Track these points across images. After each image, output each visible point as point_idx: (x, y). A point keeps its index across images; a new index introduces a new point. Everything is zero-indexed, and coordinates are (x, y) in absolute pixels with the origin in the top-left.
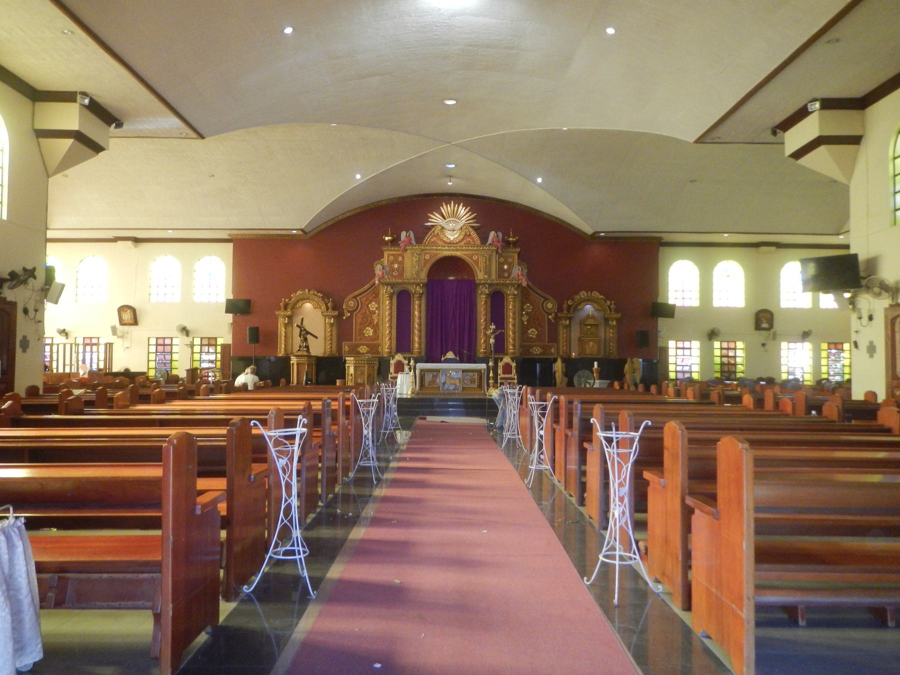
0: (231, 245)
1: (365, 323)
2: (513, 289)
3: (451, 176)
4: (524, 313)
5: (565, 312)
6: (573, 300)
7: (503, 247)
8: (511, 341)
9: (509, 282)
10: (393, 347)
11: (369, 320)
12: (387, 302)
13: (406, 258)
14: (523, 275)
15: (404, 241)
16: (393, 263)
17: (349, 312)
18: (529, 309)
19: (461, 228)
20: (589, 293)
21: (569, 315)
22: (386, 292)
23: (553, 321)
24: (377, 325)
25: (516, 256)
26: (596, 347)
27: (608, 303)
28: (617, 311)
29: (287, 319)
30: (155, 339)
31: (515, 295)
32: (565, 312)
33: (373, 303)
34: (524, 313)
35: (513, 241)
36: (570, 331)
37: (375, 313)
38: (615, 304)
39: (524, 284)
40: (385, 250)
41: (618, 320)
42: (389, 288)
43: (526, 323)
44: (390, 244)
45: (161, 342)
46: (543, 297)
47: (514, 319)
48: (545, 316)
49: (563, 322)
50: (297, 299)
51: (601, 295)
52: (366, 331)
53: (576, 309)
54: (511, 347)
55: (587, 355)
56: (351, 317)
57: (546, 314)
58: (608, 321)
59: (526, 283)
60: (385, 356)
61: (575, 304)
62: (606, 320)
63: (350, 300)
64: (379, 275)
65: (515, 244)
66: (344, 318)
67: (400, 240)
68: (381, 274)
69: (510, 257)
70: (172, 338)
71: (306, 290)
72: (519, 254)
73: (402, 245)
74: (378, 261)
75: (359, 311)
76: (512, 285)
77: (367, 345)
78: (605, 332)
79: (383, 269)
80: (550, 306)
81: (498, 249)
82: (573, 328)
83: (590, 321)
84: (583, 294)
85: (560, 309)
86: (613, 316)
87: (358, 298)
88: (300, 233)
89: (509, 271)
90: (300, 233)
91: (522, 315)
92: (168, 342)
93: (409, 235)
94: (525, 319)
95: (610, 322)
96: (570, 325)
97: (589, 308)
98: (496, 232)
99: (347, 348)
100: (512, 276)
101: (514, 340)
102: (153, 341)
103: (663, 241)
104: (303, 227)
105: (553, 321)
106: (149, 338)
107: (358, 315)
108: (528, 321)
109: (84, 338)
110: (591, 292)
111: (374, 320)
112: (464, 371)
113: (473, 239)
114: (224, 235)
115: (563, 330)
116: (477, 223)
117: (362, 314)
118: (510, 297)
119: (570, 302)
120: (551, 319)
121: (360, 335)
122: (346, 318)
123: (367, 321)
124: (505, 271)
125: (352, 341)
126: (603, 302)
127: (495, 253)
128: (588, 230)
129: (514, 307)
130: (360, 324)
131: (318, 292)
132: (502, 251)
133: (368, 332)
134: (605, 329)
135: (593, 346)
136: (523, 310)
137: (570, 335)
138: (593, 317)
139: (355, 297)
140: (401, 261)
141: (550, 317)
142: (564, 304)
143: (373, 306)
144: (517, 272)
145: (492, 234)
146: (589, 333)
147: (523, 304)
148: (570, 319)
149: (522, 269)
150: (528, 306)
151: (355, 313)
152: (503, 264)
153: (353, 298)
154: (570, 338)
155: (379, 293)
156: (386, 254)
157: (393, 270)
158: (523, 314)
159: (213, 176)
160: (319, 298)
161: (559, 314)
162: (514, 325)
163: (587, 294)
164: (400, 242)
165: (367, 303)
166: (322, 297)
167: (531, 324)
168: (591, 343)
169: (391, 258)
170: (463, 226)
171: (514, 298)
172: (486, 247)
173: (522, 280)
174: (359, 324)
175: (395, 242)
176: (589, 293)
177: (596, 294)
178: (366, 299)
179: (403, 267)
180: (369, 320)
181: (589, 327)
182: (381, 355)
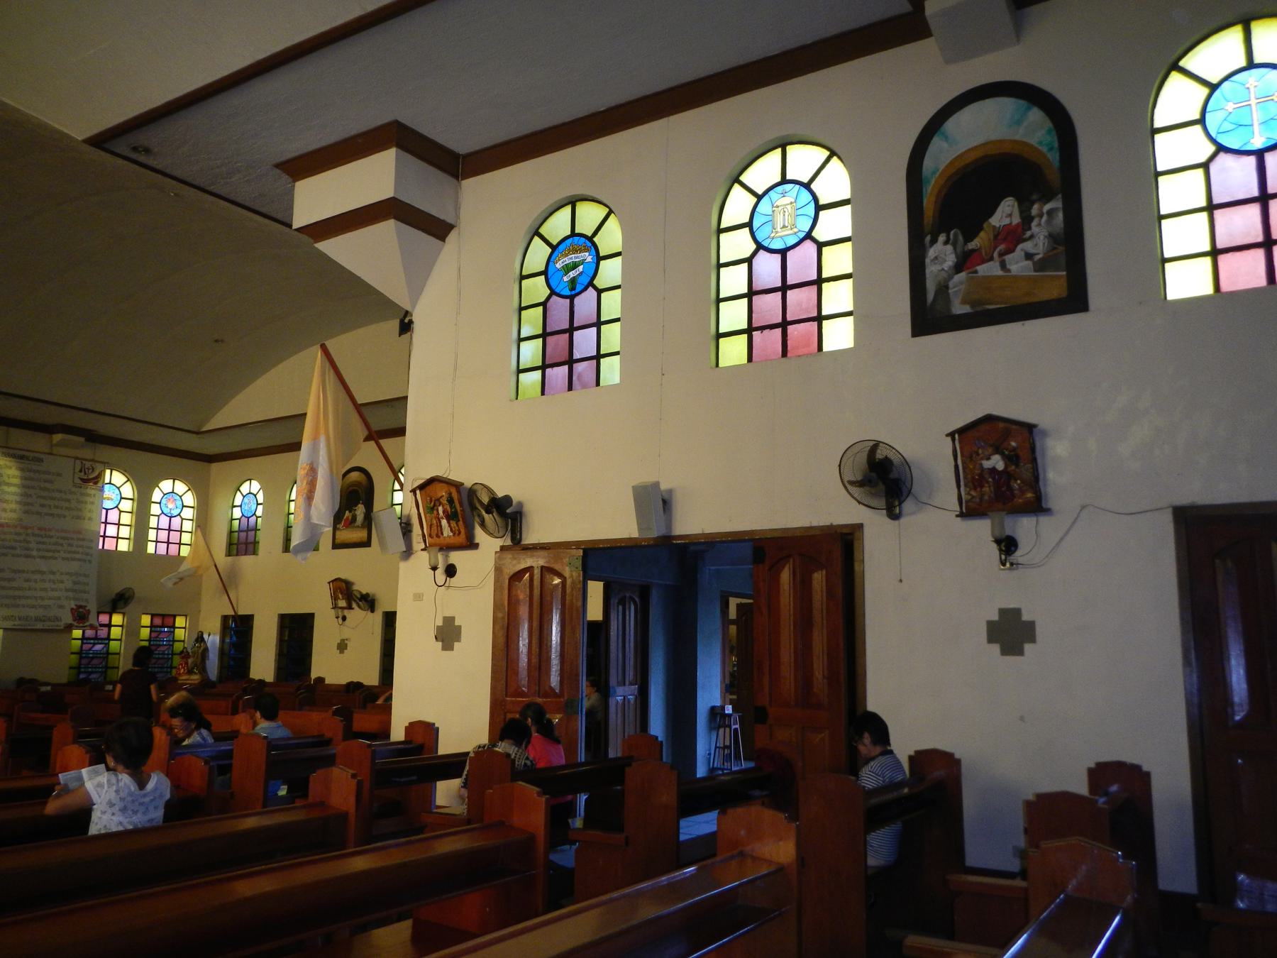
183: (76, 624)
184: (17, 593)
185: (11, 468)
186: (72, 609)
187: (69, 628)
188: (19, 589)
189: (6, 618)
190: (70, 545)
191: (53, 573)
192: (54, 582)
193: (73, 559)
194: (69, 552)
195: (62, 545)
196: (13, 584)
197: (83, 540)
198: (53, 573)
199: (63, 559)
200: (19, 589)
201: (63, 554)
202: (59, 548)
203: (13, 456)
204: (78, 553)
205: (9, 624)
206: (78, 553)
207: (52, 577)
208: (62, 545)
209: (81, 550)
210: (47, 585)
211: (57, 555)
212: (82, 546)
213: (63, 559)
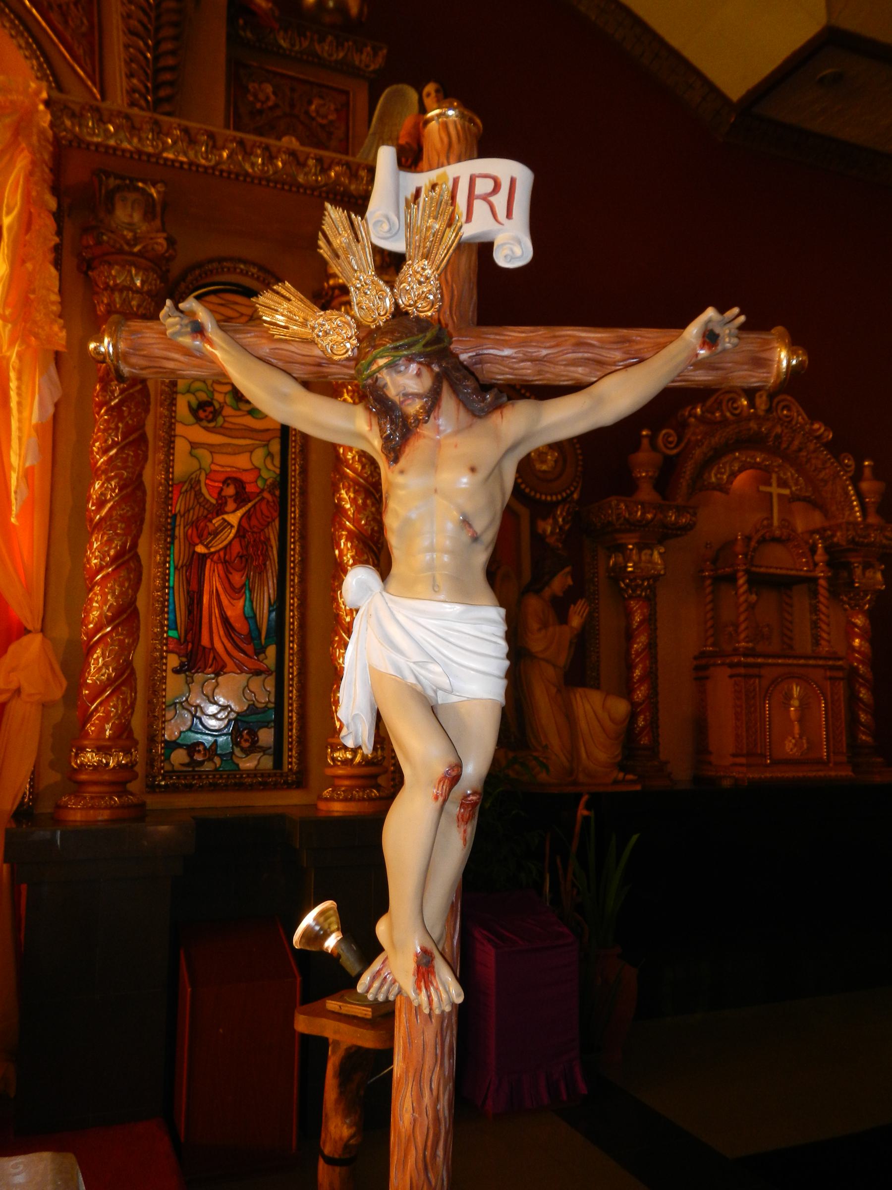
6: (681, 427)
21: (672, 517)
32: (646, 493)
38: (877, 474)
51: (813, 418)
55: (776, 762)
115: (629, 615)
120: (551, 541)
141: (546, 527)
142: (637, 447)
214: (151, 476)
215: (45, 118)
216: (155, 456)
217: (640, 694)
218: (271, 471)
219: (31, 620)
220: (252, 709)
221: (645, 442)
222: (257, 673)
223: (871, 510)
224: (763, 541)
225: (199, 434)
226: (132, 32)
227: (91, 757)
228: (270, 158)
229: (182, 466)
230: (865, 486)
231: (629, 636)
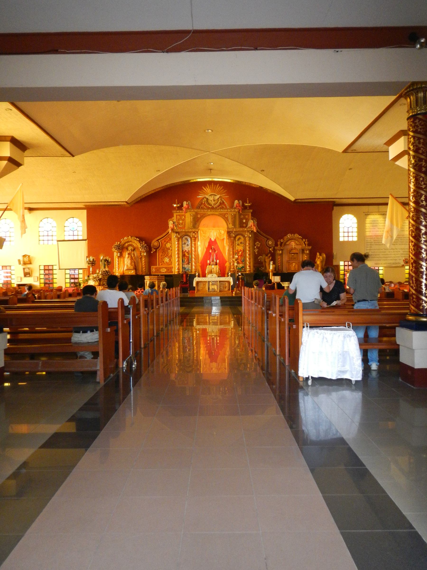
0: (85, 212)
1: (164, 255)
2: (248, 234)
3: (211, 169)
4: (255, 247)
5: (279, 246)
7: (243, 209)
8: (248, 263)
9: (247, 230)
10: (180, 269)
11: (166, 253)
12: (176, 243)
13: (187, 216)
14: (254, 226)
15: (185, 207)
16: (179, 220)
17: (154, 249)
18: (258, 245)
19: (218, 199)
20: (293, 235)
21: (281, 248)
22: (176, 237)
23: (272, 252)
24: (171, 256)
25: (250, 214)
26: (297, 266)
27: (304, 240)
28: (309, 245)
29: (119, 253)
30: (43, 266)
31: (250, 237)
32: (279, 246)
33: (168, 243)
34: (255, 247)
35: (249, 205)
36: (282, 257)
37: (169, 249)
38: (308, 241)
39: (255, 231)
40: (174, 213)
41: (310, 251)
42: (177, 235)
43: (257, 253)
44: (177, 209)
45: (47, 268)
46: (266, 238)
47: (249, 251)
48: (267, 248)
49: (278, 252)
50: (125, 242)
52: (165, 260)
53: (285, 244)
54: (248, 267)
56: (156, 252)
57: (268, 248)
58: (304, 251)
59: (256, 230)
60: (176, 274)
61: (285, 242)
62: (303, 251)
63: (155, 242)
64: (171, 227)
65: (250, 207)
66: (152, 252)
67: (183, 206)
68: (172, 227)
69: (247, 215)
70: (53, 266)
71: (130, 237)
72: (252, 213)
73: (184, 209)
74: (171, 219)
75: (160, 248)
76: (248, 231)
77: (165, 268)
78: (303, 257)
79: (173, 223)
80: (270, 243)
81: (239, 210)
82: (284, 256)
83: (294, 251)
84: (289, 236)
85: (276, 245)
86: (306, 248)
87: (159, 241)
88: (125, 203)
89: (247, 223)
90: (125, 203)
91: (254, 249)
92: (50, 268)
93: (188, 204)
94: (256, 251)
95: (305, 251)
96: (282, 254)
97: (293, 244)
98: (238, 201)
99: (154, 270)
100: (248, 227)
101: (250, 263)
102: (42, 268)
103: (336, 203)
104: (127, 200)
105: (272, 252)
106: (40, 266)
107: (160, 250)
108: (258, 252)
109: (2, 266)
110: (294, 234)
111: (169, 253)
112: (220, 282)
113: (225, 205)
114: (81, 206)
116: (227, 196)
117: (162, 250)
118: (247, 238)
119: (282, 241)
121: (161, 262)
122: (153, 252)
123: (165, 254)
124: (244, 223)
125: (157, 265)
126: (301, 240)
127: (238, 213)
128: (292, 199)
129: (249, 244)
130: (161, 256)
131: (137, 237)
132: (242, 212)
133: (166, 260)
134: (303, 255)
135: (295, 265)
136: (255, 245)
137: (282, 260)
138: (295, 249)
139: (158, 240)
140: (184, 219)
141: (271, 249)
142: (278, 242)
143: (168, 245)
144: (251, 224)
145: (236, 202)
146: (293, 258)
147: (255, 242)
148: (282, 250)
149: (254, 222)
150: (258, 243)
151: (158, 250)
152: (242, 219)
153: (157, 241)
154: (282, 261)
155: (171, 237)
156: (175, 215)
157: (179, 224)
158: (255, 248)
159: (75, 172)
160: (137, 241)
161: (276, 248)
162: (249, 255)
163: (292, 235)
164: (183, 208)
165: (165, 243)
166: (139, 241)
167: (260, 254)
168: (294, 264)
169: (178, 217)
170: (219, 198)
171: (249, 239)
172: (233, 210)
173: (253, 228)
174: (160, 256)
175: (180, 208)
176: (293, 235)
177: (297, 235)
178: (164, 241)
179: (185, 222)
180: (166, 253)
181: (293, 255)
182: (174, 274)
183: (405, 264)
184: (387, 256)
185: (381, 218)
186: (404, 260)
187: (403, 266)
188: (387, 255)
189: (385, 264)
190: (401, 240)
191: (396, 249)
192: (397, 252)
193: (403, 244)
194: (401, 242)
195: (398, 240)
196: (385, 253)
197: (405, 238)
198: (396, 249)
199: (399, 244)
200: (387, 255)
201: (399, 243)
202: (398, 241)
203: (381, 214)
204: (404, 242)
205: (385, 265)
206: (404, 242)
207: (396, 250)
208: (398, 240)
209: (405, 241)
210: (395, 253)
211: (397, 243)
212: (405, 240)
213: (399, 244)
214: (235, 251)
215: (227, 230)
216: (234, 249)
217: (279, 264)
218: (243, 249)
219: (227, 261)
220: (242, 267)
221: (279, 241)
222: (243, 264)
223: (307, 245)
224: (292, 249)
225: (238, 246)
226: (231, 219)
227: (232, 269)
228: (241, 229)
229: (237, 249)
230: (306, 242)
231: (278, 259)
